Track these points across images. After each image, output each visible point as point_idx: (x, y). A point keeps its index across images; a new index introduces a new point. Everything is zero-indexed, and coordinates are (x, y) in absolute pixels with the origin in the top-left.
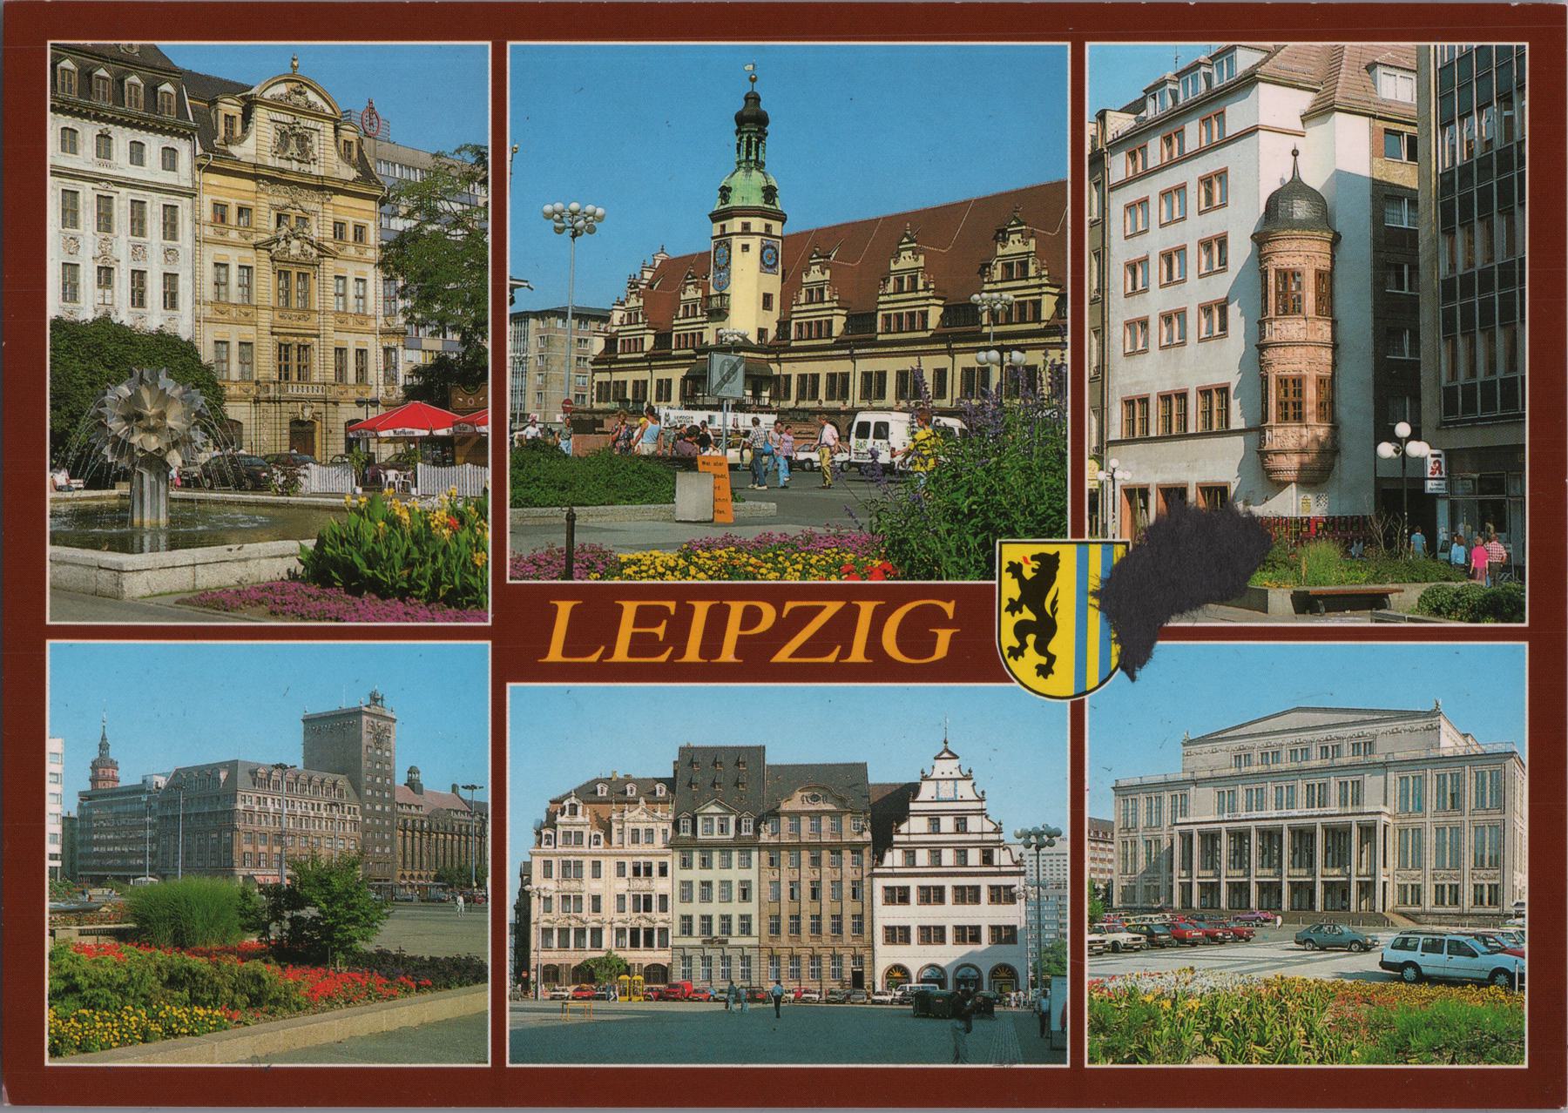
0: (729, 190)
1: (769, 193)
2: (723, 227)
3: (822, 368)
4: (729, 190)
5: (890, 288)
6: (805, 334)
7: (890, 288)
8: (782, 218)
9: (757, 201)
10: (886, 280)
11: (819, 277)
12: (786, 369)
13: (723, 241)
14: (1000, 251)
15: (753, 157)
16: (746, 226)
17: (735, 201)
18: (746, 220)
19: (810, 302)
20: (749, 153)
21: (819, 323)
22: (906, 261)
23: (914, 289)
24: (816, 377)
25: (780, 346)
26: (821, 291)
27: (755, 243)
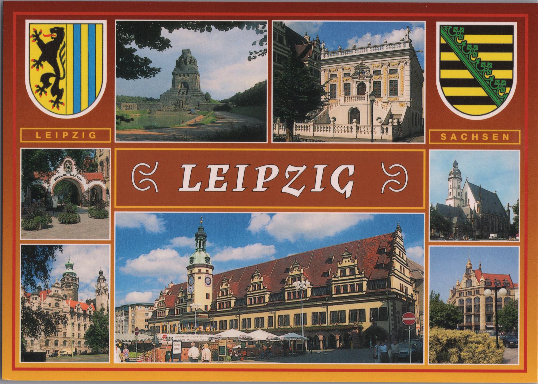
0: (193, 258)
1: (207, 259)
4: (193, 258)
5: (251, 289)
6: (222, 307)
7: (251, 289)
8: (212, 268)
9: (203, 262)
13: (191, 275)
14: (290, 274)
15: (202, 247)
16: (200, 270)
17: (196, 262)
18: (200, 268)
19: (223, 295)
20: (200, 246)
22: (256, 280)
23: (260, 289)
25: (213, 311)
26: (227, 292)
27: (203, 276)
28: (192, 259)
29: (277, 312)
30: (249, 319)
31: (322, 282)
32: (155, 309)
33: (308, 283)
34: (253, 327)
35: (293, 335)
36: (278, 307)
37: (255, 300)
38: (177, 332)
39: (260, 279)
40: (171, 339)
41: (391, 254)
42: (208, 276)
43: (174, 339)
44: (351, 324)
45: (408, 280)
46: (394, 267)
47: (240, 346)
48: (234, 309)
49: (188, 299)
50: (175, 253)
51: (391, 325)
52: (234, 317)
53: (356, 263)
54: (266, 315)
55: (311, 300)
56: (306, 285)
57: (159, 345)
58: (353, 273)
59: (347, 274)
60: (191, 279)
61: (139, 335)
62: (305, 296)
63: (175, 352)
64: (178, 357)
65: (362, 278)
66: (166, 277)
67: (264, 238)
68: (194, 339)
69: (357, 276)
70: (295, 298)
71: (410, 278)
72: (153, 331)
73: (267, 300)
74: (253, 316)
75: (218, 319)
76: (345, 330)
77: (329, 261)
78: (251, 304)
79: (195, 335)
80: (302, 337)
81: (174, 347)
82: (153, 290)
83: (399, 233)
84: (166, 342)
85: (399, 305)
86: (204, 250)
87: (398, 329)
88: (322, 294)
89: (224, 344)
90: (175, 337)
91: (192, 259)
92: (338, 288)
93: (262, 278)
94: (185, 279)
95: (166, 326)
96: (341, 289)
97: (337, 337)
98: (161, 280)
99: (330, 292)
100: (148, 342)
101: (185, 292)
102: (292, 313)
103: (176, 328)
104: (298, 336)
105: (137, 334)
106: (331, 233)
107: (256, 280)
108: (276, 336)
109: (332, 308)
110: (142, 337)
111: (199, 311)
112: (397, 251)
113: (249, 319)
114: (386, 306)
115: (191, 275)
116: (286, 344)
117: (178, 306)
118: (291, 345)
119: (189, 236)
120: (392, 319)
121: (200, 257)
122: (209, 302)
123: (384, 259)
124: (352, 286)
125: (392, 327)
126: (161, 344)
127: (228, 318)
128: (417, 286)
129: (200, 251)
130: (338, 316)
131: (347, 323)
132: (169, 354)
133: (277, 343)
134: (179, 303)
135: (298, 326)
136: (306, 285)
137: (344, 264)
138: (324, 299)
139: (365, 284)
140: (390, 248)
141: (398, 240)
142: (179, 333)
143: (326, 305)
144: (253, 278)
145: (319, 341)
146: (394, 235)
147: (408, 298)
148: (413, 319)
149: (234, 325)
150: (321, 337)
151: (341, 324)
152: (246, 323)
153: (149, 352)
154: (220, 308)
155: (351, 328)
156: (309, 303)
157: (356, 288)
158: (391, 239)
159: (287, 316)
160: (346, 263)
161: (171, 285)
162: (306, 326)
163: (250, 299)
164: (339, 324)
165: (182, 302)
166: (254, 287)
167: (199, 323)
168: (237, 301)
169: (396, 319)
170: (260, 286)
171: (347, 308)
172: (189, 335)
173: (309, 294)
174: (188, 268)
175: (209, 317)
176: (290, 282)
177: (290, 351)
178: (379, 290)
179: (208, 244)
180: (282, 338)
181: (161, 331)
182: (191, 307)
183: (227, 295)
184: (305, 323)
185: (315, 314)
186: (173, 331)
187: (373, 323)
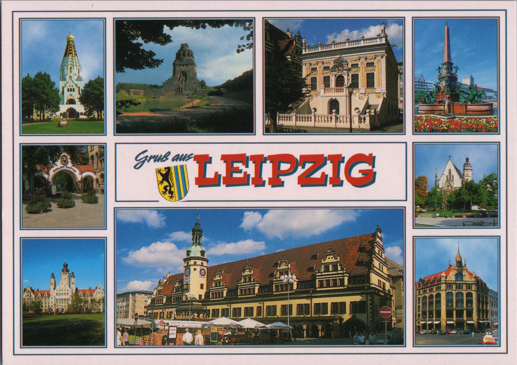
0: (190, 251)
1: (203, 253)
4: (190, 251)
5: (242, 281)
8: (207, 261)
9: (199, 255)
10: (241, 279)
11: (219, 278)
13: (188, 267)
14: (278, 268)
15: (198, 241)
16: (195, 263)
17: (192, 255)
18: (195, 261)
19: (216, 286)
20: (196, 241)
21: (219, 293)
22: (247, 273)
23: (250, 281)
25: (206, 300)
26: (220, 283)
27: (198, 268)
28: (188, 252)
29: (265, 302)
30: (240, 309)
31: (308, 276)
32: (153, 297)
33: (294, 277)
34: (242, 316)
35: (280, 324)
36: (266, 298)
37: (245, 291)
38: (173, 318)
39: (251, 272)
40: (168, 324)
41: (371, 252)
42: (204, 268)
43: (170, 325)
44: (332, 315)
45: (386, 276)
46: (373, 265)
47: (230, 333)
48: (226, 299)
49: (184, 288)
50: (173, 246)
51: (369, 317)
52: (225, 306)
53: (339, 260)
54: (255, 305)
55: (296, 293)
56: (293, 279)
57: (156, 330)
58: (335, 268)
59: (330, 270)
60: (188, 270)
61: (138, 320)
62: (292, 289)
63: (171, 337)
64: (174, 341)
65: (344, 273)
66: (164, 268)
67: (256, 234)
68: (188, 325)
69: (339, 272)
70: (282, 291)
71: (388, 275)
72: (151, 317)
73: (256, 291)
74: (243, 306)
75: (210, 308)
76: (326, 322)
77: (314, 257)
78: (241, 295)
79: (190, 322)
80: (288, 326)
81: (170, 332)
82: (152, 280)
83: (379, 234)
84: (163, 327)
85: (377, 299)
86: (199, 244)
87: (375, 321)
88: (307, 287)
89: (215, 330)
90: (171, 322)
91: (188, 252)
92: (321, 282)
93: (252, 271)
94: (182, 270)
95: (164, 313)
96: (325, 283)
97: (320, 327)
98: (160, 270)
99: (314, 286)
100: (147, 327)
101: (181, 282)
102: (279, 304)
103: (173, 315)
104: (284, 325)
105: (136, 319)
106: (317, 231)
107: (247, 273)
108: (262, 325)
109: (316, 301)
110: (141, 322)
111: (193, 300)
112: (377, 250)
113: (240, 309)
114: (365, 300)
115: (188, 267)
116: (273, 332)
117: (174, 294)
118: (277, 333)
119: (186, 231)
120: (370, 313)
121: (196, 251)
122: (203, 292)
123: (364, 257)
124: (335, 281)
125: (370, 319)
126: (158, 329)
127: (220, 307)
128: (393, 283)
129: (196, 245)
130: (321, 308)
131: (329, 315)
132: (165, 339)
133: (265, 331)
134: (176, 292)
135: (285, 316)
136: (293, 279)
137: (328, 260)
138: (308, 292)
139: (346, 279)
140: (370, 247)
141: (378, 240)
142: (175, 319)
143: (311, 297)
144: (244, 270)
145: (303, 330)
146: (374, 235)
147: (385, 293)
148: (390, 312)
149: (225, 313)
150: (305, 327)
151: (323, 315)
152: (237, 313)
153: (147, 336)
154: (213, 298)
155: (332, 319)
156: (295, 296)
157: (338, 283)
158: (371, 239)
159: (275, 307)
160: (330, 259)
161: (169, 275)
162: (292, 316)
163: (241, 290)
164: (321, 315)
165: (179, 291)
166: (245, 279)
167: (193, 311)
168: (229, 291)
169: (374, 312)
170: (250, 279)
171: (329, 301)
172: (184, 322)
173: (295, 287)
174: (185, 260)
175: (202, 305)
176: (278, 276)
177: (276, 339)
178: (358, 285)
179: (203, 239)
180: (269, 326)
181: (158, 317)
182: (186, 296)
183: (220, 286)
184: (291, 313)
185: (299, 306)
186: (169, 317)
187: (353, 315)
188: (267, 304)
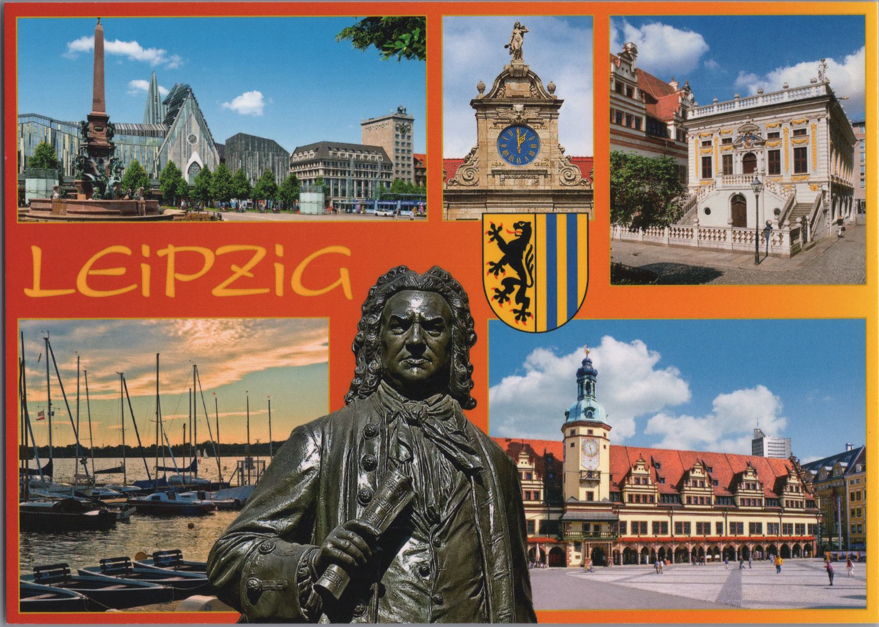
0: (593, 409)
2: (590, 432)
3: (650, 519)
12: (622, 518)
24: (644, 524)
188: (731, 519)
